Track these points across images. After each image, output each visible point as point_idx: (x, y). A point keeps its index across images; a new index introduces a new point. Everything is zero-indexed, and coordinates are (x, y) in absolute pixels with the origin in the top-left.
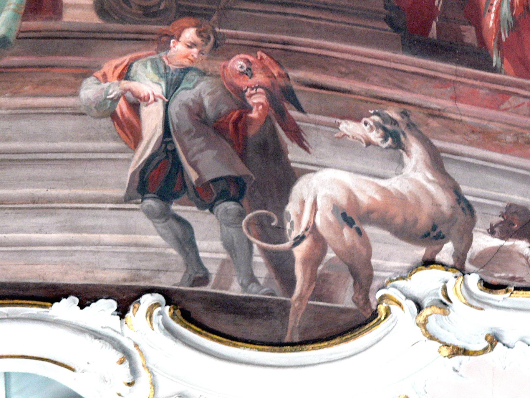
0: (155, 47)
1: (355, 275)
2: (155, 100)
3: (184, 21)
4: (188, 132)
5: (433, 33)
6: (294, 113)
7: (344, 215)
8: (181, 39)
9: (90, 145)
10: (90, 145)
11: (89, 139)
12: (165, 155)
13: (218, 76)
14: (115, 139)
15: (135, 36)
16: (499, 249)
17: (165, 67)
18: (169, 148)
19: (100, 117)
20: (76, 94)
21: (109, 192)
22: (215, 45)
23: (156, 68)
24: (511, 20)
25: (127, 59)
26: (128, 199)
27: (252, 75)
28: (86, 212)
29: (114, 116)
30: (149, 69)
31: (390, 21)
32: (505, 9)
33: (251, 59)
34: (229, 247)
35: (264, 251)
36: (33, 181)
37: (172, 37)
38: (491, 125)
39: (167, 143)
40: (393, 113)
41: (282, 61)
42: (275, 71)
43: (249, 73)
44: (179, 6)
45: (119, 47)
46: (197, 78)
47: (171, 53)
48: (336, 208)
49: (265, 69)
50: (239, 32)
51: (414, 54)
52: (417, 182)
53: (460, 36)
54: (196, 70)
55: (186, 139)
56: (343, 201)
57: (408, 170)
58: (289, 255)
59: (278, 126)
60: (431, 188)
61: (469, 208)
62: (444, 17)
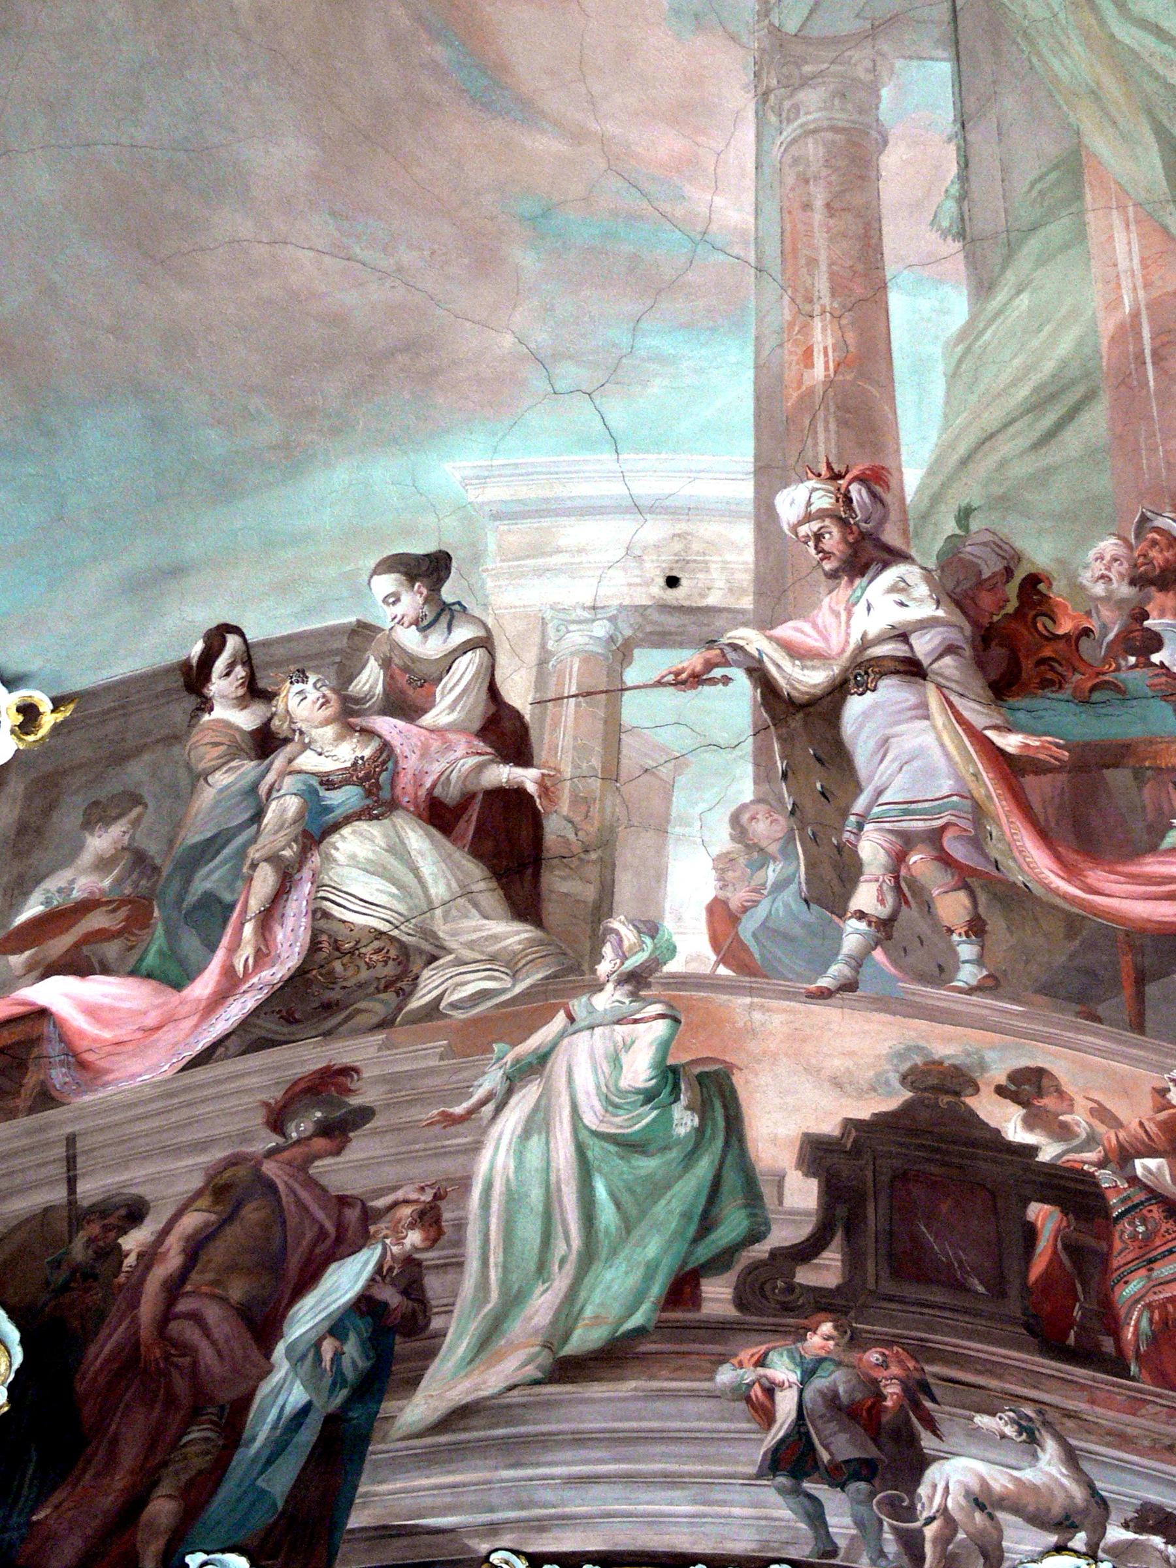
0: (792, 1338)
1: (985, 1555)
2: (790, 1387)
3: (821, 1316)
4: (821, 1417)
5: (1071, 1340)
6: (929, 1404)
7: (976, 1501)
8: (818, 1332)
9: (724, 1426)
10: (724, 1426)
11: (723, 1419)
12: (797, 1437)
13: (854, 1367)
14: (749, 1421)
15: (773, 1328)
16: (1132, 1543)
17: (801, 1356)
18: (802, 1430)
19: (734, 1400)
20: (712, 1379)
21: (740, 1469)
22: (852, 1338)
23: (792, 1358)
24: (1150, 1333)
25: (763, 1348)
26: (760, 1475)
27: (887, 1368)
28: (718, 1488)
29: (748, 1399)
30: (785, 1359)
31: (1027, 1326)
32: (1144, 1323)
33: (887, 1352)
34: (859, 1523)
35: (895, 1530)
36: (664, 1457)
37: (810, 1330)
38: (1129, 1430)
39: (800, 1426)
40: (1028, 1411)
41: (919, 1357)
42: (911, 1364)
43: (885, 1365)
44: (817, 1302)
45: (755, 1337)
46: (832, 1368)
47: (807, 1344)
48: (968, 1493)
49: (901, 1362)
50: (875, 1328)
51: (1052, 1359)
52: (1051, 1477)
53: (1098, 1345)
54: (831, 1360)
55: (819, 1423)
56: (975, 1486)
57: (1042, 1464)
58: (920, 1532)
59: (911, 1414)
60: (1065, 1481)
61: (1103, 1503)
62: (1082, 1327)
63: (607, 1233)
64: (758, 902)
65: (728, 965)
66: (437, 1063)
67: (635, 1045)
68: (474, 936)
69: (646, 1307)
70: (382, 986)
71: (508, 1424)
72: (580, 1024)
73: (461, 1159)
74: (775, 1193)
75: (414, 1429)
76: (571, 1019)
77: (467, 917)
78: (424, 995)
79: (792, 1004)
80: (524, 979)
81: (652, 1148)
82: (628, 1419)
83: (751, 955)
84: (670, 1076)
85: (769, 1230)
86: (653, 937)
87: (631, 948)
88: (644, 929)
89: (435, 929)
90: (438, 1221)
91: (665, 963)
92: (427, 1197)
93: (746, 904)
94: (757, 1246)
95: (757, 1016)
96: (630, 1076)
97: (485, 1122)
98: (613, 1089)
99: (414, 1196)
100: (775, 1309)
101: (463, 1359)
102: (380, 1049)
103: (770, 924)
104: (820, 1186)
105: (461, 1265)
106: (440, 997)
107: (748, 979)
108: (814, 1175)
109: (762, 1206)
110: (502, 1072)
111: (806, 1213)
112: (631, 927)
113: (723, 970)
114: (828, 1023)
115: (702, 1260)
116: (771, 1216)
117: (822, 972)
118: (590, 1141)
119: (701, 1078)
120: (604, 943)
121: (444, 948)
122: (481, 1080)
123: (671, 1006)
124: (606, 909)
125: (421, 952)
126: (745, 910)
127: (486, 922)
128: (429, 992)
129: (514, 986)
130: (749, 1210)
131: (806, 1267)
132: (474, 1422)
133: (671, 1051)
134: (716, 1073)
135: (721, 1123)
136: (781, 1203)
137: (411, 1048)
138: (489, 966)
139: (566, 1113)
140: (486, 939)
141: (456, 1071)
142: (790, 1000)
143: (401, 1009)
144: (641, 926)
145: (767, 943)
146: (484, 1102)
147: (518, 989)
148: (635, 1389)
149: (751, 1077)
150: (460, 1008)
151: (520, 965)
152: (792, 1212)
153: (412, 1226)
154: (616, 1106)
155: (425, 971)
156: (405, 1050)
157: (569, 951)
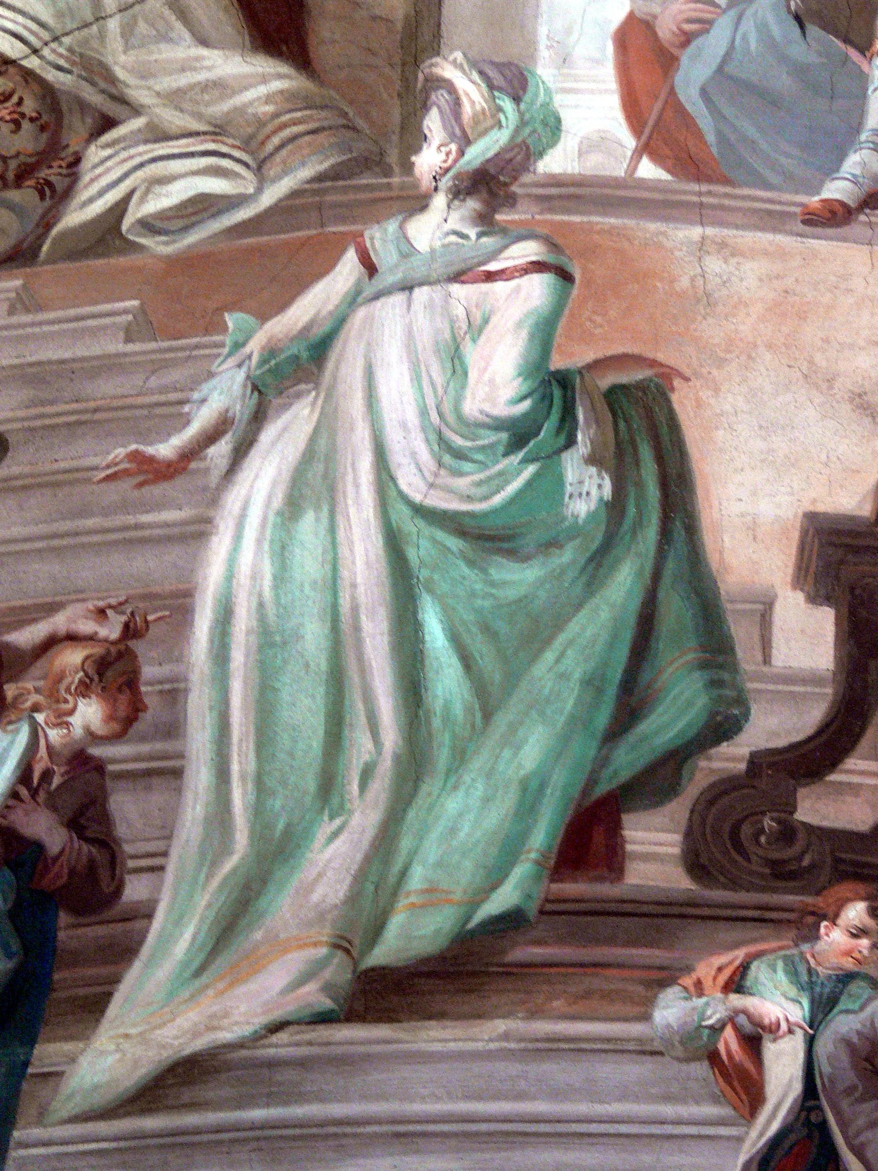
0: (793, 933)
2: (790, 1031)
3: (844, 889)
4: (849, 1091)
8: (841, 921)
9: (668, 1110)
10: (668, 1110)
11: (667, 1098)
12: (805, 1132)
14: (715, 1100)
15: (756, 914)
17: (810, 971)
18: (813, 1118)
19: (688, 1060)
20: (646, 1017)
23: (793, 973)
25: (740, 954)
29: (713, 1057)
30: (781, 975)
37: (824, 917)
39: (810, 1110)
44: (838, 861)
45: (726, 933)
46: (867, 992)
47: (820, 946)
54: (867, 977)
55: (845, 1104)
63: (447, 718)
64: (710, 23)
65: (657, 158)
66: (121, 347)
67: (490, 327)
68: (183, 80)
69: (521, 871)
70: (11, 175)
71: (270, 1099)
72: (387, 278)
73: (174, 554)
74: (756, 637)
75: (98, 1100)
76: (371, 268)
77: (170, 40)
78: (91, 200)
79: (780, 238)
80: (278, 178)
81: (529, 542)
82: (497, 1097)
83: (699, 135)
84: (557, 393)
85: (746, 715)
86: (517, 100)
87: (476, 119)
88: (498, 80)
89: (109, 60)
90: (131, 683)
91: (541, 154)
92: (111, 630)
93: (687, 27)
94: (724, 748)
95: (714, 265)
96: (482, 391)
97: (214, 478)
98: (451, 418)
99: (86, 627)
100: (762, 876)
101: (185, 964)
102: (12, 311)
103: (729, 69)
104: (838, 624)
105: (177, 773)
106: (120, 208)
107: (695, 187)
108: (828, 600)
109: (733, 667)
110: (241, 376)
111: (813, 679)
112: (475, 76)
113: (648, 170)
114: (845, 277)
115: (625, 775)
116: (750, 685)
117: (831, 170)
118: (411, 526)
119: (614, 395)
120: (425, 107)
121: (121, 100)
122: (206, 388)
123: (553, 245)
124: (428, 37)
125: (83, 106)
126: (687, 39)
127: (204, 52)
128: (101, 193)
129: (259, 190)
130: (706, 675)
131: (817, 788)
132: (209, 1092)
133: (557, 340)
134: (642, 387)
135: (653, 492)
136: (767, 659)
137: (72, 312)
138: (211, 146)
139: (366, 463)
140: (205, 87)
141: (158, 366)
142: (775, 230)
143: (48, 227)
144: (492, 73)
145: (728, 111)
146: (211, 437)
147: (270, 197)
148: (506, 1036)
149: (705, 394)
150: (159, 232)
151: (270, 147)
152: (789, 678)
153: (84, 689)
154: (459, 455)
155: (93, 148)
156: (60, 314)
157: (360, 123)
